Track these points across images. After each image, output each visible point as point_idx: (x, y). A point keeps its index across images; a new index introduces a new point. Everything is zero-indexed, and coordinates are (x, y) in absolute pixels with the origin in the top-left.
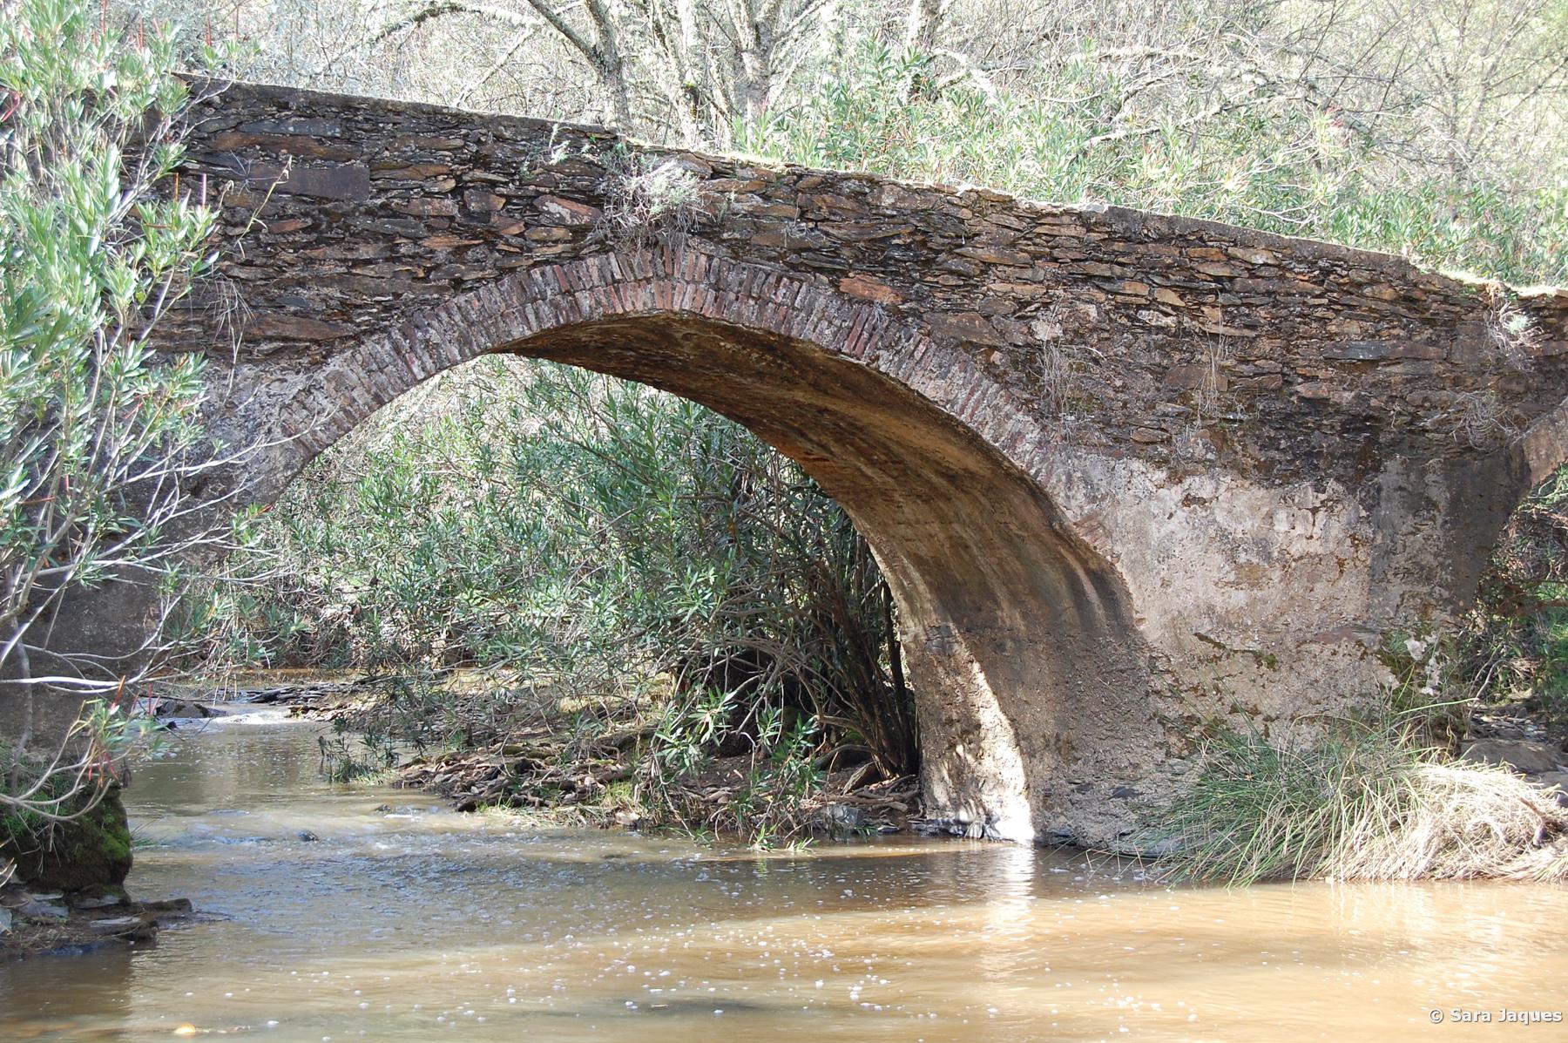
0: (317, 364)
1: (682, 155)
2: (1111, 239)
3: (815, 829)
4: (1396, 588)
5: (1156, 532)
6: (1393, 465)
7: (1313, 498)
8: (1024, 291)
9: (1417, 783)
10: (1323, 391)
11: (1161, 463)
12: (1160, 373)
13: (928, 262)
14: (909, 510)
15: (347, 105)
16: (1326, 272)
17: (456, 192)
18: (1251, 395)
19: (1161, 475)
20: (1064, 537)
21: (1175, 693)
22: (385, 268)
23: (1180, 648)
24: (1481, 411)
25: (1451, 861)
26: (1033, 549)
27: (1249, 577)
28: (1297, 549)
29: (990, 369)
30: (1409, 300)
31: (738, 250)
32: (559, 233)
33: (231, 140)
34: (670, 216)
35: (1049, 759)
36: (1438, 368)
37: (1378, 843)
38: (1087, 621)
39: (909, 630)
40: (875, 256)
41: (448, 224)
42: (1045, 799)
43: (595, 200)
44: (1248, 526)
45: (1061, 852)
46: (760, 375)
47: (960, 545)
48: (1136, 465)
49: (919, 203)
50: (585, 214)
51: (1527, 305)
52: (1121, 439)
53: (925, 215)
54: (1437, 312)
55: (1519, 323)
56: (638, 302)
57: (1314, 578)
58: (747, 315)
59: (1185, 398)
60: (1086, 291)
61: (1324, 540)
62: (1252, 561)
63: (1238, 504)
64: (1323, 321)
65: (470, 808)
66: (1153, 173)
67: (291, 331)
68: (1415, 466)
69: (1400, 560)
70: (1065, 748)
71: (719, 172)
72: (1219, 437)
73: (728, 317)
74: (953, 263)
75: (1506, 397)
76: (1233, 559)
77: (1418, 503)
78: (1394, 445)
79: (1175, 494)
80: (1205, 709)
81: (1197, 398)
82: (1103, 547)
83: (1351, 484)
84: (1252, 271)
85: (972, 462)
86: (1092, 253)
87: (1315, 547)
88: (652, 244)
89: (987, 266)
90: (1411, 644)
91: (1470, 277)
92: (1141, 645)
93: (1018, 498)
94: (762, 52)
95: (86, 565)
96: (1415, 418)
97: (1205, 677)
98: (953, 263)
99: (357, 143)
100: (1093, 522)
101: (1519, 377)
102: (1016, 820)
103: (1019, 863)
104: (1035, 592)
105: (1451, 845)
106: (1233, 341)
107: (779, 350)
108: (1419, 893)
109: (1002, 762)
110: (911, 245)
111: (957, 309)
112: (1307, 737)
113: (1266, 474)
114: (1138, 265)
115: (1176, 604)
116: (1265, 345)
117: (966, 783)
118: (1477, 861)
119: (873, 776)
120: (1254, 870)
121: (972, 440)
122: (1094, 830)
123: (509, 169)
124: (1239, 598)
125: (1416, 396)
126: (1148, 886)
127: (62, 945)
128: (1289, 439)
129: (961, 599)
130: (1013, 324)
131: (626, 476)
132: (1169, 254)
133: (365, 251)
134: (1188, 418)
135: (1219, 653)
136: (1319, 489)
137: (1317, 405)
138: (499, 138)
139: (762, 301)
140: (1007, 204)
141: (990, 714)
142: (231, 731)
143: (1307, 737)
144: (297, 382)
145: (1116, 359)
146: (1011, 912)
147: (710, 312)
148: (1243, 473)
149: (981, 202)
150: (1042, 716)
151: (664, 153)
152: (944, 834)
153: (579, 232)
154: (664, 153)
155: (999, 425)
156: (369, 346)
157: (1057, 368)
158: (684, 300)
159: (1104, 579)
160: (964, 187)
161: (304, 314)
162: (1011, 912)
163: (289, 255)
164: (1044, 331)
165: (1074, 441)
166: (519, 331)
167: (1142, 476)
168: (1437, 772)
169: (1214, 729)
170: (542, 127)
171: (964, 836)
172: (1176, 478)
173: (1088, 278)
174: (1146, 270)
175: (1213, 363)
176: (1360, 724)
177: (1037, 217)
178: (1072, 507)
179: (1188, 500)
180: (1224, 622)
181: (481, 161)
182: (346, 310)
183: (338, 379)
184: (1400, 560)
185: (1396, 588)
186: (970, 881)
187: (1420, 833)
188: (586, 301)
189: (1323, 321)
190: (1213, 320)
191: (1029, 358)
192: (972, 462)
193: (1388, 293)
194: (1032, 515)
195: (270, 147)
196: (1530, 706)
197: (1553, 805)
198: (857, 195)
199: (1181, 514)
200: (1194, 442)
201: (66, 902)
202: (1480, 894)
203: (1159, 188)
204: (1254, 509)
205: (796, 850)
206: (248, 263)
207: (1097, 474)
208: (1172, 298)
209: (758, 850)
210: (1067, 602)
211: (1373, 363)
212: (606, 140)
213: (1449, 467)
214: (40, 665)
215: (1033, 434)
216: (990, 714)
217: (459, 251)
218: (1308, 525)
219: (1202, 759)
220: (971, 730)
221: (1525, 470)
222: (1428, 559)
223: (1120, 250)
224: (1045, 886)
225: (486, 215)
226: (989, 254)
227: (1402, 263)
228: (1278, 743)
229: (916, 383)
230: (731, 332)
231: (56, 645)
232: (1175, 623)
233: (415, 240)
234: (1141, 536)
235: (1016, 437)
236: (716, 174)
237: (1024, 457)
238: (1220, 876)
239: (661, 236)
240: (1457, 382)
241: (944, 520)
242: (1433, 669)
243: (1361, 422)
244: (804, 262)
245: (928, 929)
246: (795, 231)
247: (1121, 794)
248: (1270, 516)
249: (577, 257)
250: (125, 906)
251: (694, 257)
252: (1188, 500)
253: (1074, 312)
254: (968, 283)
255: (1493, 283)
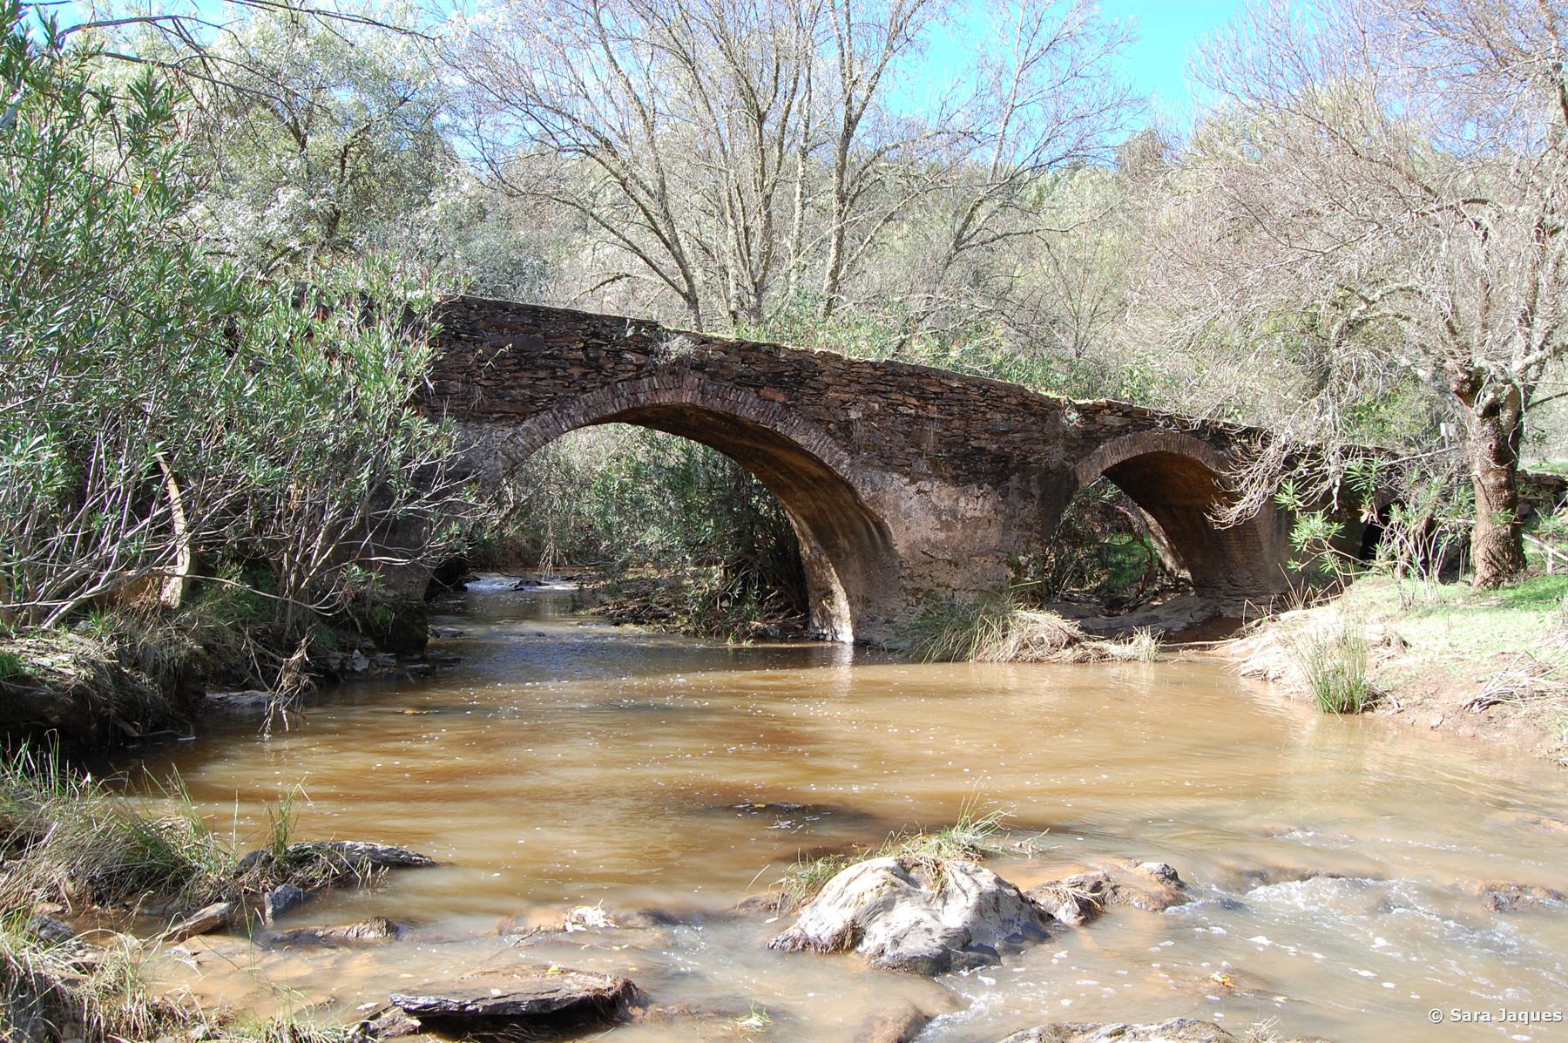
0: (519, 424)
1: (687, 334)
2: (886, 374)
3: (761, 636)
4: (1015, 533)
5: (903, 506)
6: (1015, 478)
7: (977, 492)
8: (845, 397)
9: (1014, 618)
10: (983, 444)
11: (906, 475)
12: (907, 435)
13: (801, 384)
14: (799, 495)
15: (535, 309)
16: (986, 391)
17: (583, 349)
18: (949, 445)
19: (906, 480)
20: (862, 507)
21: (911, 578)
22: (551, 382)
23: (914, 557)
24: (1056, 455)
25: (1025, 653)
26: (851, 513)
27: (947, 526)
28: (969, 515)
29: (828, 431)
30: (1024, 405)
31: (713, 376)
32: (630, 367)
33: (482, 324)
34: (680, 361)
35: (860, 606)
36: (1037, 435)
37: (994, 646)
38: (874, 545)
39: (805, 550)
40: (776, 380)
41: (578, 363)
42: (857, 625)
43: (646, 353)
44: (946, 504)
45: (865, 649)
46: (727, 433)
47: (821, 511)
48: (895, 475)
49: (797, 357)
50: (643, 359)
51: (1078, 408)
52: (888, 463)
53: (800, 362)
54: (1040, 411)
55: (1074, 416)
56: (666, 398)
57: (977, 528)
58: (716, 405)
59: (918, 446)
60: (873, 397)
61: (982, 511)
62: (948, 519)
63: (942, 494)
64: (984, 413)
65: (617, 624)
66: (916, 347)
67: (506, 409)
68: (1025, 479)
69: (1017, 520)
70: (866, 602)
71: (706, 341)
72: (934, 464)
73: (707, 406)
74: (812, 384)
75: (1068, 448)
76: (939, 518)
77: (1026, 495)
78: (1016, 470)
79: (913, 488)
80: (926, 585)
81: (924, 446)
82: (878, 512)
83: (995, 486)
84: (952, 390)
85: (821, 473)
86: (877, 380)
87: (978, 514)
88: (673, 373)
89: (828, 385)
90: (1021, 558)
91: (1052, 395)
92: (894, 555)
93: (842, 489)
94: (758, 295)
95: (398, 510)
96: (1026, 457)
97: (925, 570)
98: (812, 384)
99: (539, 326)
100: (874, 500)
101: (1074, 440)
102: (846, 634)
103: (847, 654)
104: (853, 532)
105: (1026, 646)
106: (942, 421)
107: (732, 420)
108: (1010, 670)
109: (842, 605)
110: (792, 375)
111: (814, 404)
112: (971, 598)
113: (955, 481)
114: (899, 387)
115: (913, 537)
116: (956, 423)
117: (827, 618)
118: (1037, 654)
119: (794, 613)
120: (935, 656)
121: (820, 463)
122: (877, 638)
123: (609, 340)
124: (942, 535)
125: (1026, 447)
126: (891, 662)
127: (388, 675)
128: (964, 465)
129: (824, 535)
130: (839, 411)
131: (681, 480)
132: (913, 382)
133: (542, 374)
134: (920, 455)
135: (931, 560)
136: (980, 487)
137: (981, 450)
138: (604, 325)
139: (723, 399)
140: (838, 358)
141: (837, 588)
142: (550, 592)
143: (971, 598)
144: (509, 432)
145: (887, 428)
146: (844, 672)
147: (699, 403)
148: (945, 480)
149: (825, 356)
150: (860, 588)
151: (679, 333)
152: (817, 639)
153: (640, 367)
154: (679, 333)
155: (832, 456)
156: (542, 415)
157: (859, 432)
158: (687, 398)
159: (880, 526)
160: (817, 351)
161: (513, 401)
162: (844, 672)
163: (507, 375)
164: (853, 415)
165: (866, 464)
166: (612, 410)
167: (898, 481)
168: (1022, 614)
169: (929, 593)
170: (624, 320)
171: (824, 640)
172: (913, 481)
173: (875, 392)
174: (902, 388)
175: (932, 430)
176: (996, 593)
177: (852, 364)
178: (865, 494)
179: (919, 492)
180: (934, 546)
181: (596, 335)
182: (533, 400)
183: (528, 430)
184: (1017, 520)
185: (1015, 533)
186: (827, 659)
187: (1012, 642)
188: (642, 398)
189: (984, 413)
190: (933, 411)
191: (847, 426)
192: (821, 473)
193: (1014, 401)
194: (848, 496)
195: (500, 327)
196: (1098, 589)
197: (1075, 630)
198: (768, 353)
199: (916, 498)
200: (923, 466)
201: (397, 657)
202: (1040, 668)
203: (921, 352)
204: (950, 496)
205: (747, 644)
206: (488, 379)
207: (877, 479)
208: (914, 401)
209: (730, 643)
210: (865, 537)
211: (1006, 433)
212: (653, 326)
213: (1041, 480)
214: (380, 552)
215: (848, 461)
216: (837, 588)
217: (584, 375)
218: (974, 504)
219: (921, 608)
220: (829, 594)
221: (1076, 481)
222: (1030, 520)
223: (891, 379)
224: (856, 662)
225: (597, 359)
226: (829, 380)
227: (1021, 388)
228: (958, 601)
229: (794, 437)
230: (710, 413)
231: (389, 543)
232: (912, 546)
233: (564, 369)
234: (897, 507)
235: (840, 462)
236: (704, 342)
237: (844, 470)
238: (918, 659)
239: (680, 368)
240: (1045, 442)
241: (814, 500)
242: (1031, 569)
243: (1001, 459)
244: (742, 382)
245: (776, 678)
246: (740, 368)
247: (888, 622)
248: (957, 500)
249: (638, 378)
250: (424, 660)
251: (693, 379)
252: (919, 492)
253: (868, 407)
254: (819, 393)
255: (1063, 398)
